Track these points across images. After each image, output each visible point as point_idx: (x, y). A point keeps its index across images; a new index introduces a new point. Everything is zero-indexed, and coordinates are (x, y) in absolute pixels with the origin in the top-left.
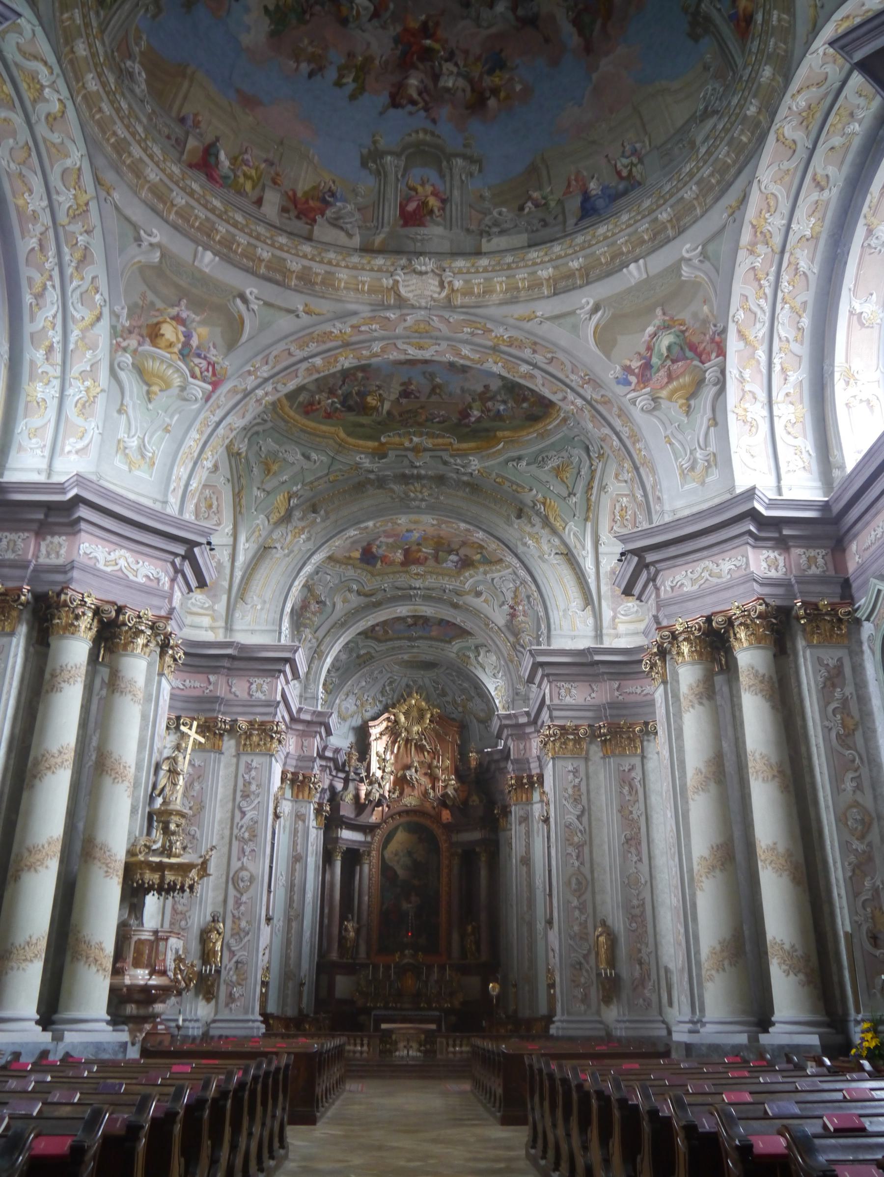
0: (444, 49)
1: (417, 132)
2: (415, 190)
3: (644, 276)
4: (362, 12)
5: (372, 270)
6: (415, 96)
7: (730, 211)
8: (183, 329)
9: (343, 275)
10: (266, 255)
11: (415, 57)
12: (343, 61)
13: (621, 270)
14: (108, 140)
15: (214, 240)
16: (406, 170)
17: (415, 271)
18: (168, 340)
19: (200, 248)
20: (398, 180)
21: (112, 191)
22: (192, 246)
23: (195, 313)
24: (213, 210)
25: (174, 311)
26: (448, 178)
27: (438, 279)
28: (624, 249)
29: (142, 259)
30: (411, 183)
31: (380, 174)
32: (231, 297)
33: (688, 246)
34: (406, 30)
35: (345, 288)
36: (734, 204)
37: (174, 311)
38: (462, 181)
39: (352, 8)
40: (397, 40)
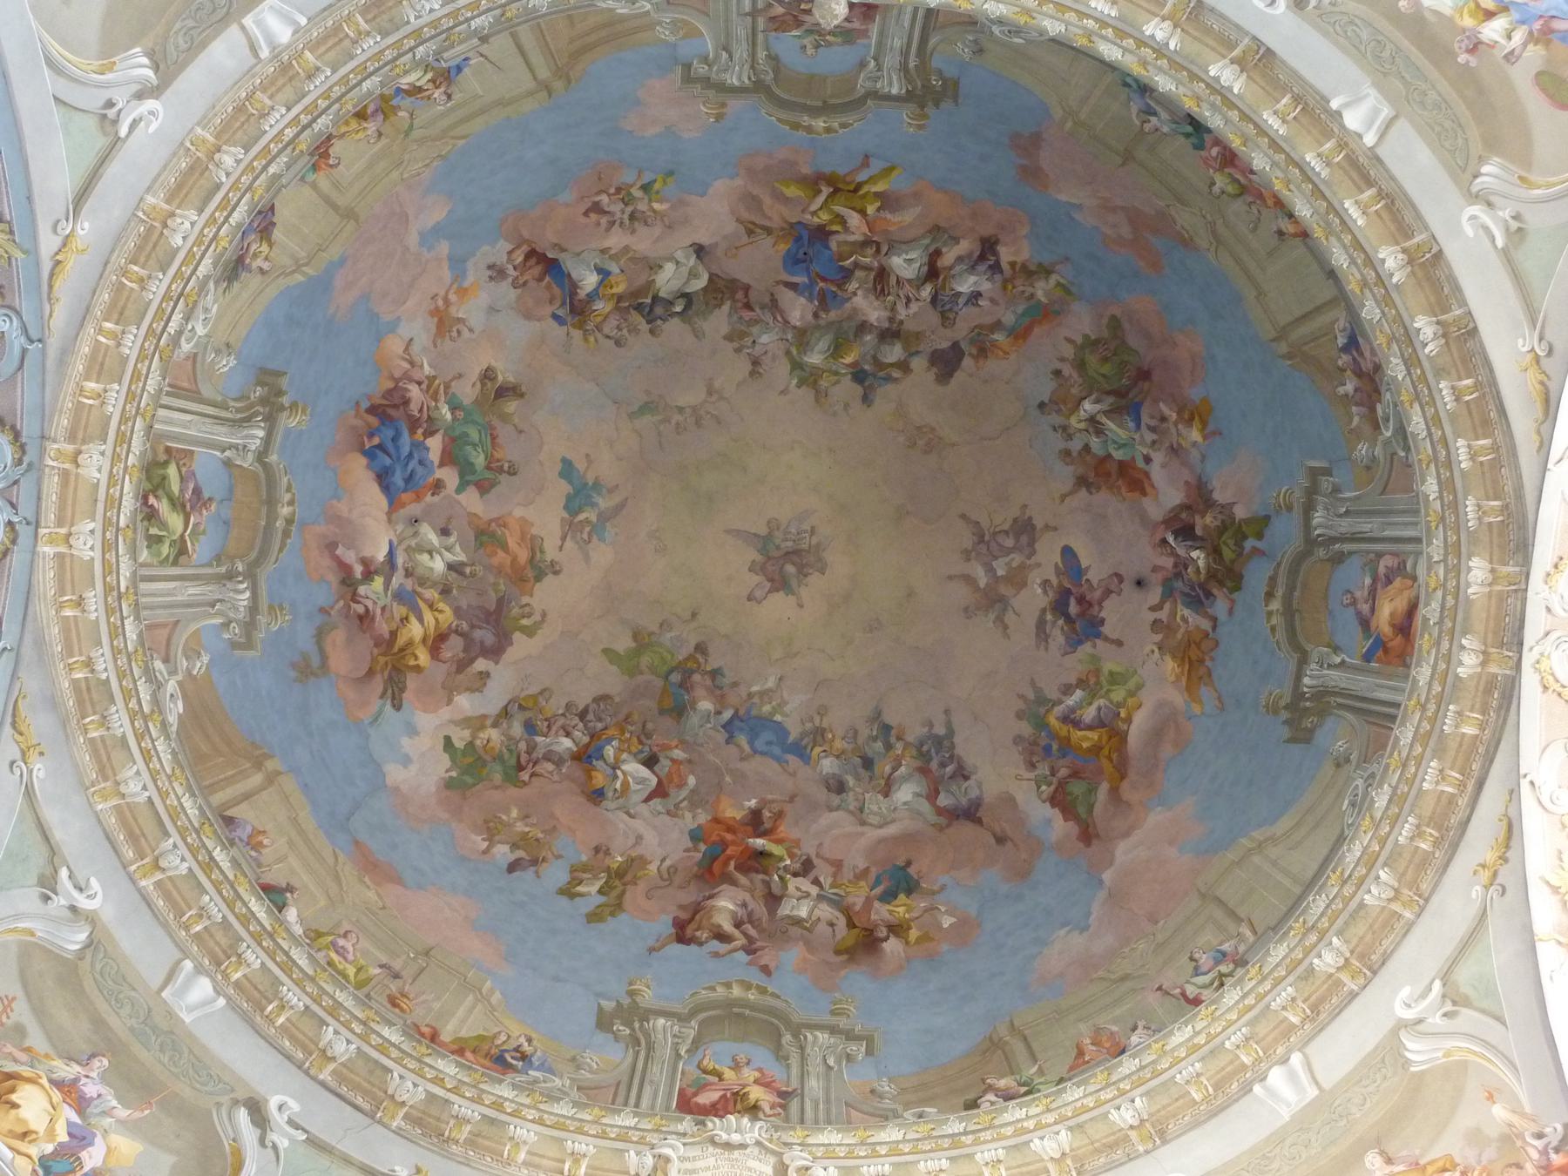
0: (792, 856)
1: (728, 985)
2: (720, 1076)
3: (1313, 1092)
4: (633, 786)
5: (603, 1136)
6: (728, 927)
7: (1485, 876)
8: (75, 1118)
9: (525, 1133)
10: (342, 1048)
11: (732, 863)
12: (584, 858)
13: (1246, 1089)
14: (70, 668)
15: (226, 976)
16: (696, 1043)
17: (712, 1141)
18: (23, 1121)
19: (188, 965)
20: (678, 1056)
21: (33, 756)
22: (178, 955)
23: (120, 1099)
24: (247, 918)
25: (68, 1071)
26: (794, 1062)
27: (772, 1160)
28: (1246, 1060)
29: (40, 929)
30: (709, 1063)
31: (641, 1043)
32: (225, 1099)
33: (1405, 992)
34: (716, 820)
35: (525, 1163)
36: (1490, 856)
37: (68, 1071)
38: (830, 1068)
39: (616, 777)
40: (696, 836)
